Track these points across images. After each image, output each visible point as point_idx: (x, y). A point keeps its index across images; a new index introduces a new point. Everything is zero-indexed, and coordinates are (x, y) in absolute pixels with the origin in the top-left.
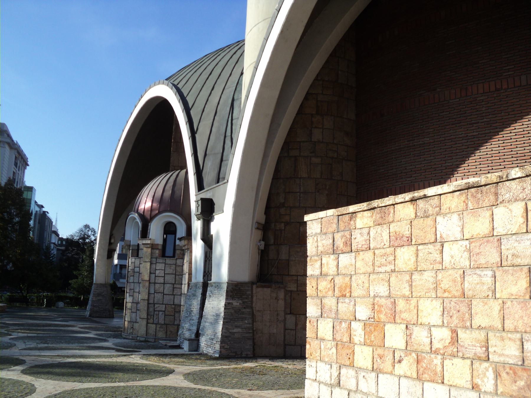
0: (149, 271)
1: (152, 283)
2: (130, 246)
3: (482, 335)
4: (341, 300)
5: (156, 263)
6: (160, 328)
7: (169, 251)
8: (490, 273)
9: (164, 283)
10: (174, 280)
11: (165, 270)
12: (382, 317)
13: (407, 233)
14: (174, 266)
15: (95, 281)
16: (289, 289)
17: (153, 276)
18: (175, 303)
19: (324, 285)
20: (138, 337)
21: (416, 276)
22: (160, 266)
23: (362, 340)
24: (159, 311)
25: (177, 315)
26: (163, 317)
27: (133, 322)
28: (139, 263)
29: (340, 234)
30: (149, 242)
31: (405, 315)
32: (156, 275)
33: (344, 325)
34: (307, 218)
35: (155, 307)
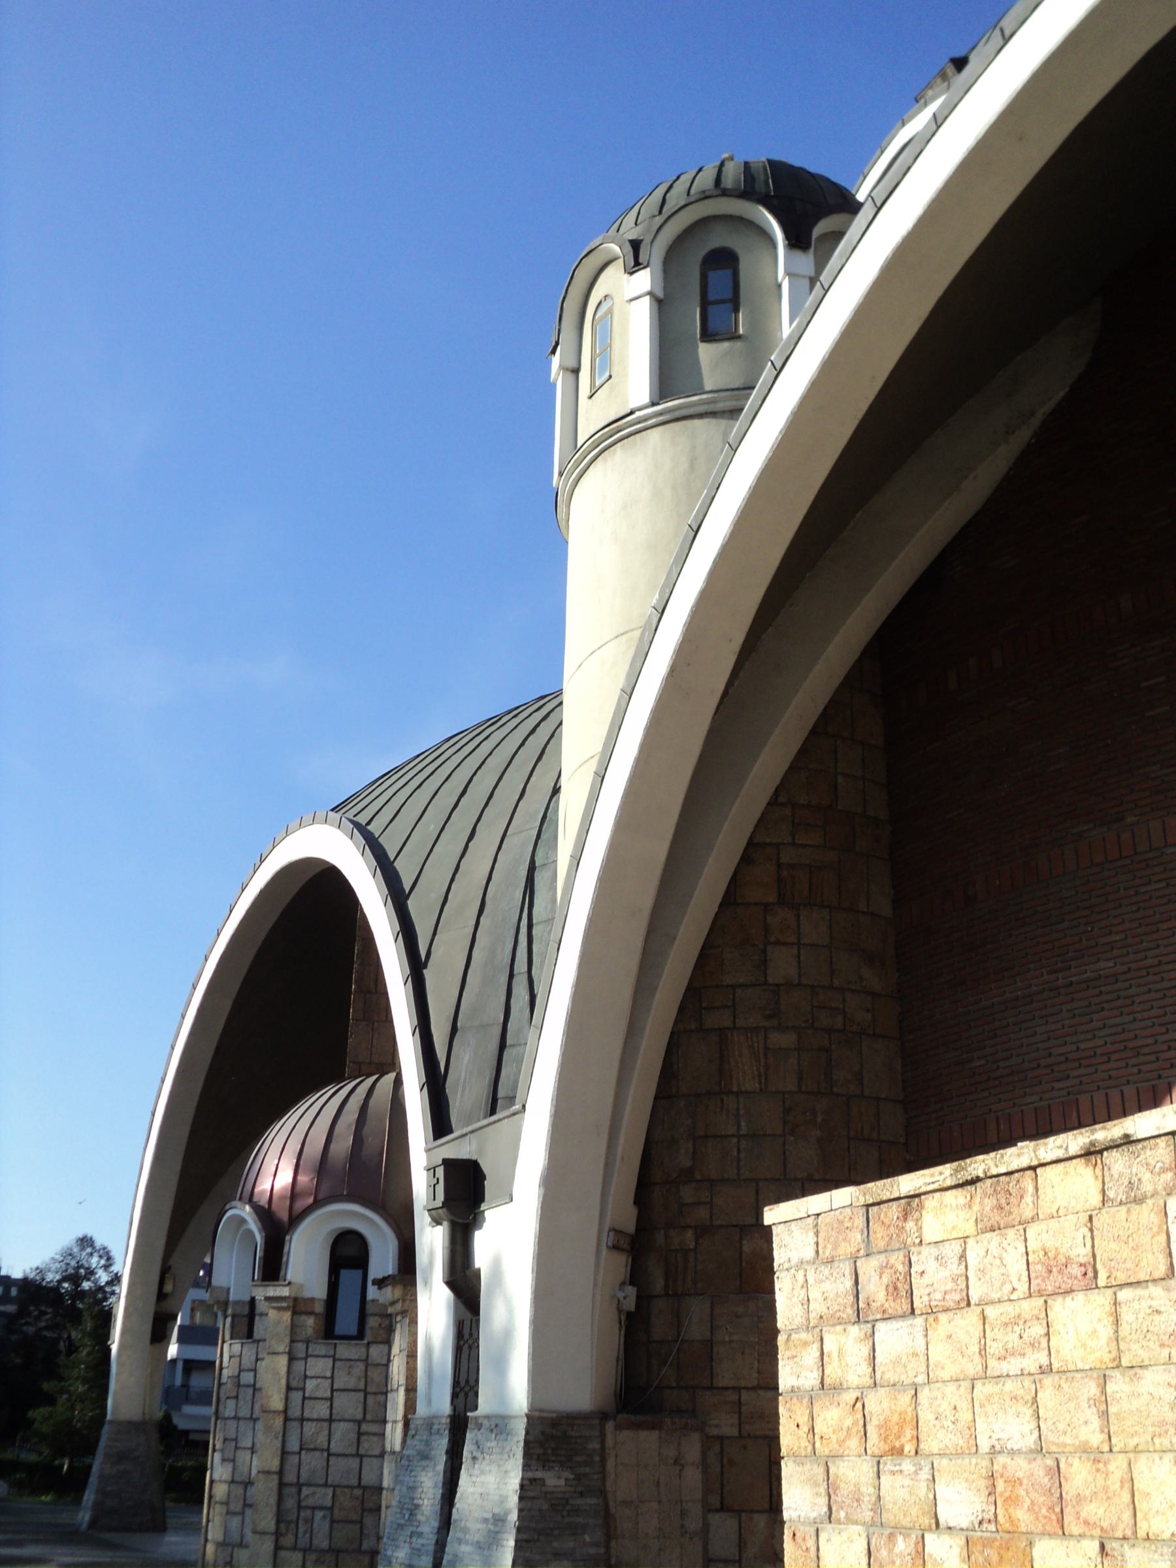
0: (284, 1382)
1: (295, 1420)
2: (226, 1303)
4: (888, 1465)
5: (307, 1356)
7: (346, 1322)
9: (331, 1420)
10: (360, 1410)
11: (332, 1377)
12: (1022, 1516)
13: (1081, 1253)
14: (361, 1366)
15: (113, 1413)
16: (715, 1432)
17: (297, 1396)
18: (363, 1483)
21: (1118, 1385)
22: (319, 1366)
24: (314, 1508)
25: (369, 1520)
26: (327, 1527)
28: (253, 1358)
29: (874, 1262)
30: (285, 1292)
31: (1094, 1510)
32: (307, 1395)
33: (902, 1545)
34: (772, 1215)
35: (302, 1497)
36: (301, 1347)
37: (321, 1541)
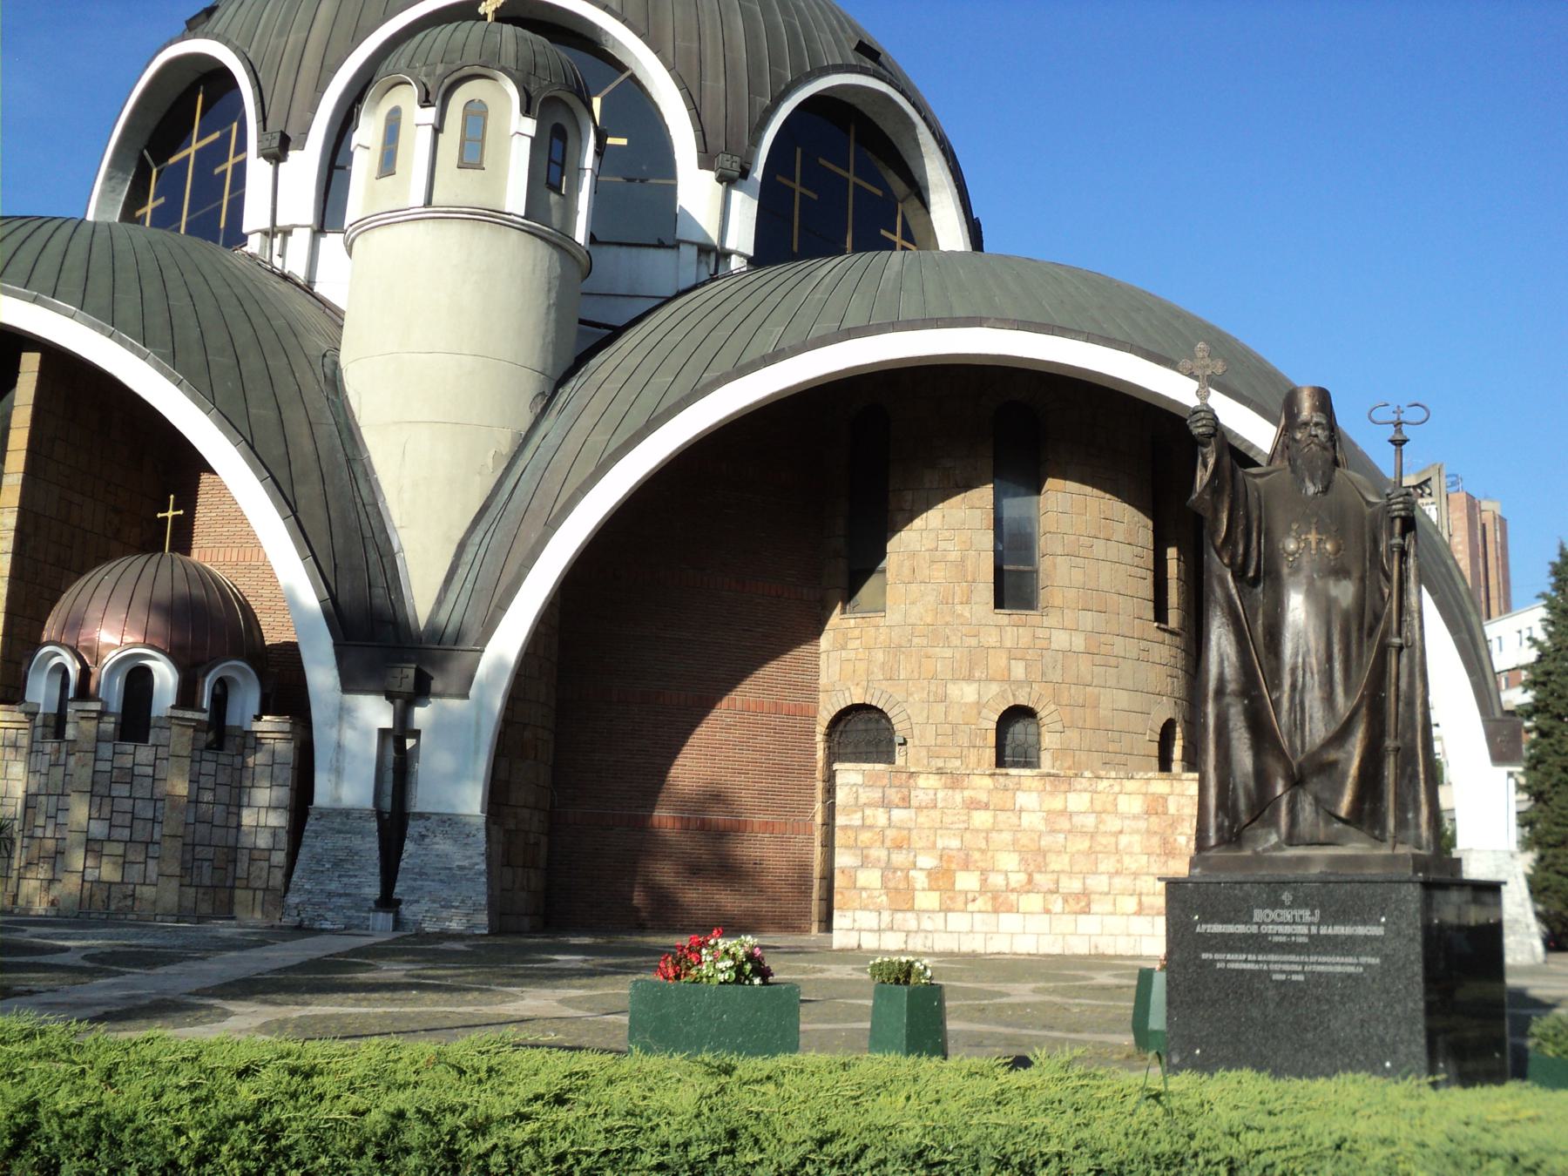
3: (1055, 876)
6: (204, 894)
8: (1062, 836)
12: (953, 866)
17: (195, 785)
19: (865, 837)
20: (157, 915)
22: (208, 767)
23: (926, 886)
24: (202, 860)
25: (230, 868)
27: (135, 885)
31: (979, 864)
36: (197, 753)
37: (207, 881)
